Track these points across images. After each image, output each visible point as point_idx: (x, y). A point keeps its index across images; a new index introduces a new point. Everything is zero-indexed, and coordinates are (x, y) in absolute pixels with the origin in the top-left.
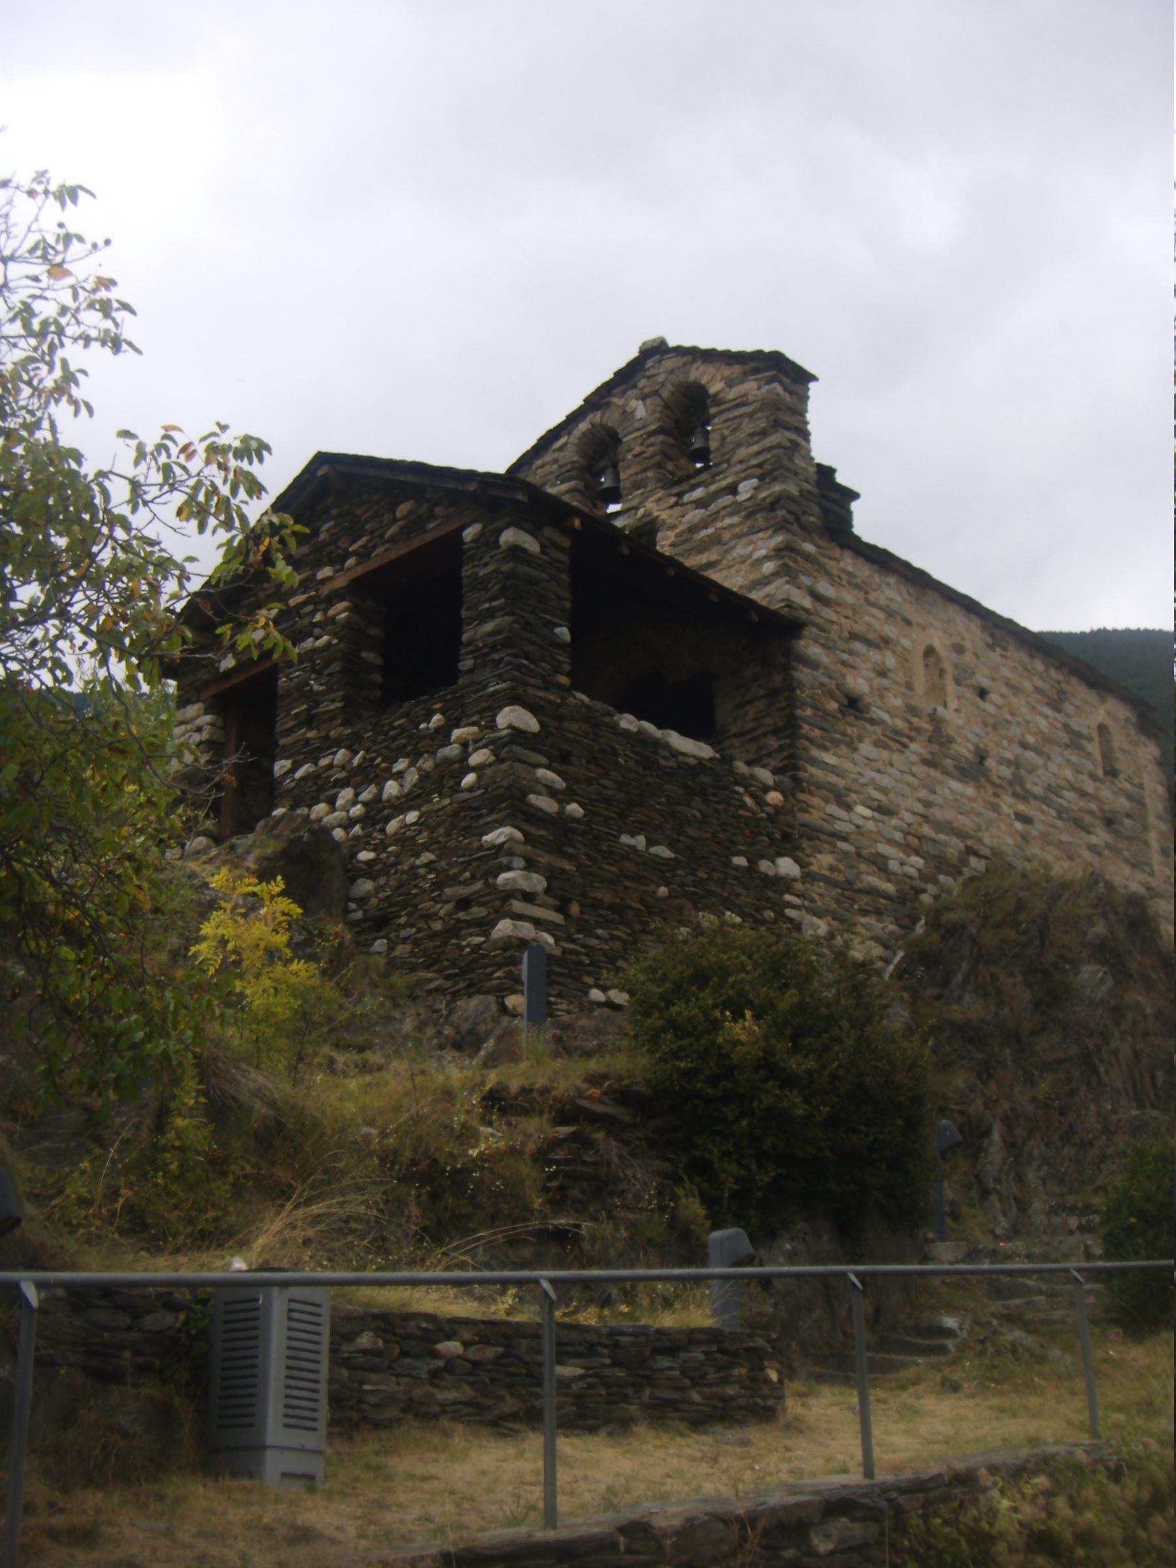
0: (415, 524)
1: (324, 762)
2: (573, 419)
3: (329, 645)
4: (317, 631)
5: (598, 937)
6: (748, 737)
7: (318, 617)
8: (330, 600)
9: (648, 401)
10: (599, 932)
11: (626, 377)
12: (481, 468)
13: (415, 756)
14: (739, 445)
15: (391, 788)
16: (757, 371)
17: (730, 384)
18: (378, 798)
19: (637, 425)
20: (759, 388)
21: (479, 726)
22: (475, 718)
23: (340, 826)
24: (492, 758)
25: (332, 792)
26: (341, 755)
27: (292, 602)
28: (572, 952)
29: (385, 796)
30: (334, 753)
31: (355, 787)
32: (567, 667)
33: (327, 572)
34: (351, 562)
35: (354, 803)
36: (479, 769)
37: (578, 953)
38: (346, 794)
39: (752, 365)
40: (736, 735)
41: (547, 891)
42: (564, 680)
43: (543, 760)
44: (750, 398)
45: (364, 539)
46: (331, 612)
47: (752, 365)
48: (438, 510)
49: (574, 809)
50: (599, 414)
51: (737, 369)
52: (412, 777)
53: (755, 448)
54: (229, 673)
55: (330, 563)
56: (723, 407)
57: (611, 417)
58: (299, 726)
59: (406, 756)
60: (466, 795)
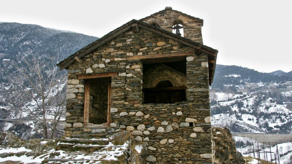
1: (132, 113)
3: (132, 77)
4: (127, 71)
7: (128, 67)
8: (132, 63)
9: (168, 20)
11: (162, 13)
13: (171, 121)
16: (196, 22)
17: (189, 22)
18: (155, 131)
19: (164, 24)
20: (197, 26)
21: (197, 119)
23: (140, 135)
25: (136, 124)
26: (139, 114)
27: (116, 59)
29: (158, 131)
30: (136, 112)
31: (146, 125)
33: (131, 54)
38: (142, 127)
39: (195, 20)
44: (195, 27)
45: (145, 48)
46: (133, 67)
47: (195, 20)
48: (174, 48)
50: (154, 19)
51: (191, 20)
52: (170, 129)
54: (89, 74)
55: (133, 52)
56: (187, 27)
58: (122, 99)
59: (167, 121)
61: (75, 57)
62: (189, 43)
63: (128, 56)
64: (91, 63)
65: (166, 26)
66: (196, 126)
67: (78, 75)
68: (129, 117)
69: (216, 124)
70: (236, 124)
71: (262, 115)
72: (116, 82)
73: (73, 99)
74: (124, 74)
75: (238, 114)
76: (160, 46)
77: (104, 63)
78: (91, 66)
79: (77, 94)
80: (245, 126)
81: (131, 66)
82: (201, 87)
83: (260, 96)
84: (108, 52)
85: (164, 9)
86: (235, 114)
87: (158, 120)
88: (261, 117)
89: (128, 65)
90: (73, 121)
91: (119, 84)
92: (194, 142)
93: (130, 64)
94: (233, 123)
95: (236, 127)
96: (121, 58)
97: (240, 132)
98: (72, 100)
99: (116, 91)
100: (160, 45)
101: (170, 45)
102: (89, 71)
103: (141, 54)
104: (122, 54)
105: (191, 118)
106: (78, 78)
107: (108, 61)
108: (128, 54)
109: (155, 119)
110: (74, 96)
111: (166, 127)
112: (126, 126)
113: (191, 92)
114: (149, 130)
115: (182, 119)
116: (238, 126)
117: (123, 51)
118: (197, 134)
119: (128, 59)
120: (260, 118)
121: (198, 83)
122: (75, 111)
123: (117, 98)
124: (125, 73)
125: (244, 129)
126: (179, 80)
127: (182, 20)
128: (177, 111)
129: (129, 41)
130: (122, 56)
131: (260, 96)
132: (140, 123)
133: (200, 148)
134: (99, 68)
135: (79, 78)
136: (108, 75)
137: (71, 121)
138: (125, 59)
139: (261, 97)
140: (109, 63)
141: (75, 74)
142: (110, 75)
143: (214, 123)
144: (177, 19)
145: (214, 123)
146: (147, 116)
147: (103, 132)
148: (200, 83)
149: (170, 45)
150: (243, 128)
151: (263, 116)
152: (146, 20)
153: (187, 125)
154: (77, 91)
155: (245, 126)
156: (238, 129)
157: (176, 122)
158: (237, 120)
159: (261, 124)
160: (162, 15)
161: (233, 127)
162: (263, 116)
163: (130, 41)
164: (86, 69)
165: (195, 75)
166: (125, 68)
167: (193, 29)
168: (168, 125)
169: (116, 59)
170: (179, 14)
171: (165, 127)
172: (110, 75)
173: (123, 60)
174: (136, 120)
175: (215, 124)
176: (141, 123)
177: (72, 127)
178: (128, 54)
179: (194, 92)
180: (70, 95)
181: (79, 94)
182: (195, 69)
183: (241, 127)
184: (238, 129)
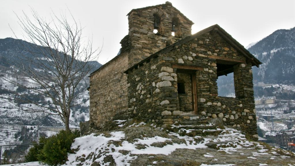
1: (215, 104)
3: (212, 73)
7: (209, 64)
9: (169, 15)
21: (250, 110)
22: (249, 108)
27: (200, 55)
30: (217, 103)
31: (224, 114)
35: (224, 117)
47: (188, 22)
51: (185, 21)
54: (181, 65)
56: (183, 27)
62: (247, 54)
63: (209, 54)
64: (182, 54)
65: (168, 21)
66: (250, 115)
67: (172, 64)
68: (213, 107)
69: (24, 116)
70: (49, 116)
71: (79, 108)
72: (203, 75)
73: (170, 87)
74: (206, 70)
75: (52, 105)
76: (226, 51)
77: (192, 57)
78: (182, 57)
79: (173, 83)
80: (59, 119)
81: (211, 64)
82: (250, 88)
83: (78, 86)
84: (193, 46)
85: (165, 3)
86: (49, 105)
87: (231, 110)
88: (78, 110)
89: (209, 62)
90: (172, 109)
91: (205, 78)
92: (249, 126)
94: (45, 115)
95: (49, 120)
96: (205, 55)
97: (53, 126)
98: (170, 88)
99: (204, 84)
100: (226, 50)
101: (232, 52)
102: (181, 61)
103: (216, 54)
104: (204, 51)
105: (247, 109)
106: (173, 66)
107: (194, 55)
108: (208, 53)
109: (229, 109)
110: (170, 84)
111: (235, 115)
112: (212, 114)
113: (245, 91)
114: (226, 118)
116: (51, 119)
117: (205, 49)
118: (250, 121)
119: (208, 57)
120: (76, 111)
121: (249, 84)
122: (173, 99)
123: (205, 89)
124: (208, 69)
125: (58, 123)
126: (179, 75)
127: (180, 19)
128: (239, 104)
130: (205, 53)
131: (78, 86)
133: (252, 131)
134: (188, 59)
135: (174, 67)
136: (196, 68)
137: (171, 109)
138: (207, 56)
139: (79, 88)
141: (169, 61)
142: (198, 69)
143: (22, 114)
144: (176, 16)
145: (22, 114)
146: (224, 107)
147: (198, 119)
148: (250, 85)
149: (232, 52)
150: (56, 122)
151: (80, 109)
152: (151, 8)
153: (245, 114)
154: (172, 79)
155: (59, 119)
156: (51, 123)
157: (240, 112)
158: (50, 112)
159: (77, 118)
160: (164, 8)
161: (44, 120)
162: (80, 109)
163: (142, 28)
164: (178, 59)
165: (247, 78)
166: (207, 64)
168: (236, 114)
169: (200, 55)
171: (234, 115)
172: (198, 68)
173: (205, 57)
174: (218, 109)
175: (22, 115)
176: (221, 111)
177: (172, 115)
178: (208, 53)
179: (246, 91)
180: (167, 82)
181: (175, 83)
182: (247, 74)
183: (54, 120)
184: (51, 123)
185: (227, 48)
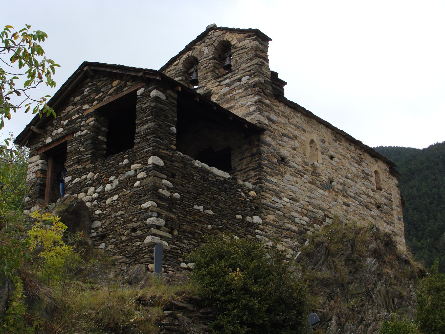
0: (119, 89)
1: (83, 177)
2: (182, 53)
3: (87, 133)
5: (185, 243)
6: (243, 171)
7: (83, 123)
8: (87, 117)
9: (209, 47)
10: (185, 241)
11: (201, 38)
12: (144, 67)
13: (117, 175)
14: (242, 63)
15: (108, 187)
16: (249, 36)
17: (239, 41)
18: (103, 191)
19: (205, 56)
22: (140, 161)
23: (89, 201)
24: (146, 175)
26: (90, 175)
27: (73, 118)
28: (174, 248)
29: (106, 190)
30: (87, 174)
31: (95, 187)
32: (175, 142)
33: (86, 106)
34: (96, 102)
35: (94, 193)
36: (141, 179)
37: (177, 249)
38: (92, 189)
39: (248, 34)
40: (239, 171)
41: (165, 226)
42: (174, 147)
43: (165, 177)
45: (101, 94)
46: (87, 122)
49: (176, 195)
50: (191, 52)
51: (242, 35)
52: (116, 183)
53: (248, 65)
54: (49, 144)
55: (88, 103)
56: (236, 50)
57: (194, 53)
58: (75, 164)
60: (136, 189)
61: (31, 127)
65: (207, 58)
93: (85, 119)
107: (66, 122)
108: (84, 108)
115: (128, 167)
129: (86, 91)
130: (78, 112)
132: (90, 186)
135: (40, 153)
140: (67, 125)
160: (203, 41)
167: (243, 51)
170: (225, 31)
185: (115, 82)
